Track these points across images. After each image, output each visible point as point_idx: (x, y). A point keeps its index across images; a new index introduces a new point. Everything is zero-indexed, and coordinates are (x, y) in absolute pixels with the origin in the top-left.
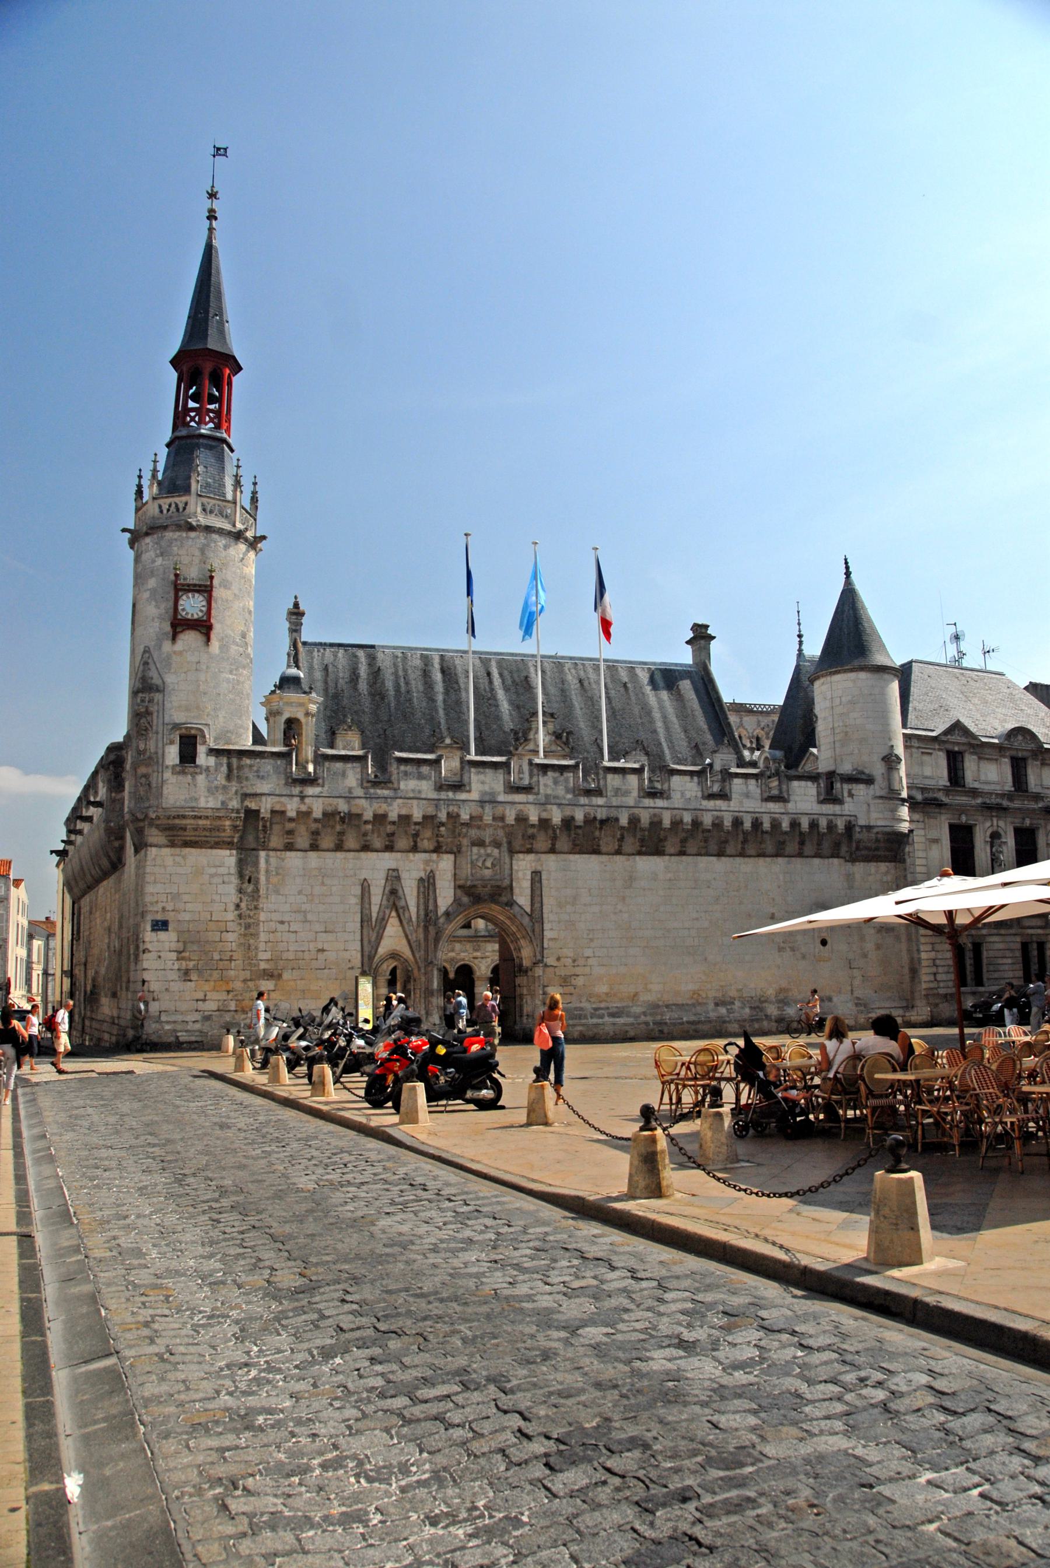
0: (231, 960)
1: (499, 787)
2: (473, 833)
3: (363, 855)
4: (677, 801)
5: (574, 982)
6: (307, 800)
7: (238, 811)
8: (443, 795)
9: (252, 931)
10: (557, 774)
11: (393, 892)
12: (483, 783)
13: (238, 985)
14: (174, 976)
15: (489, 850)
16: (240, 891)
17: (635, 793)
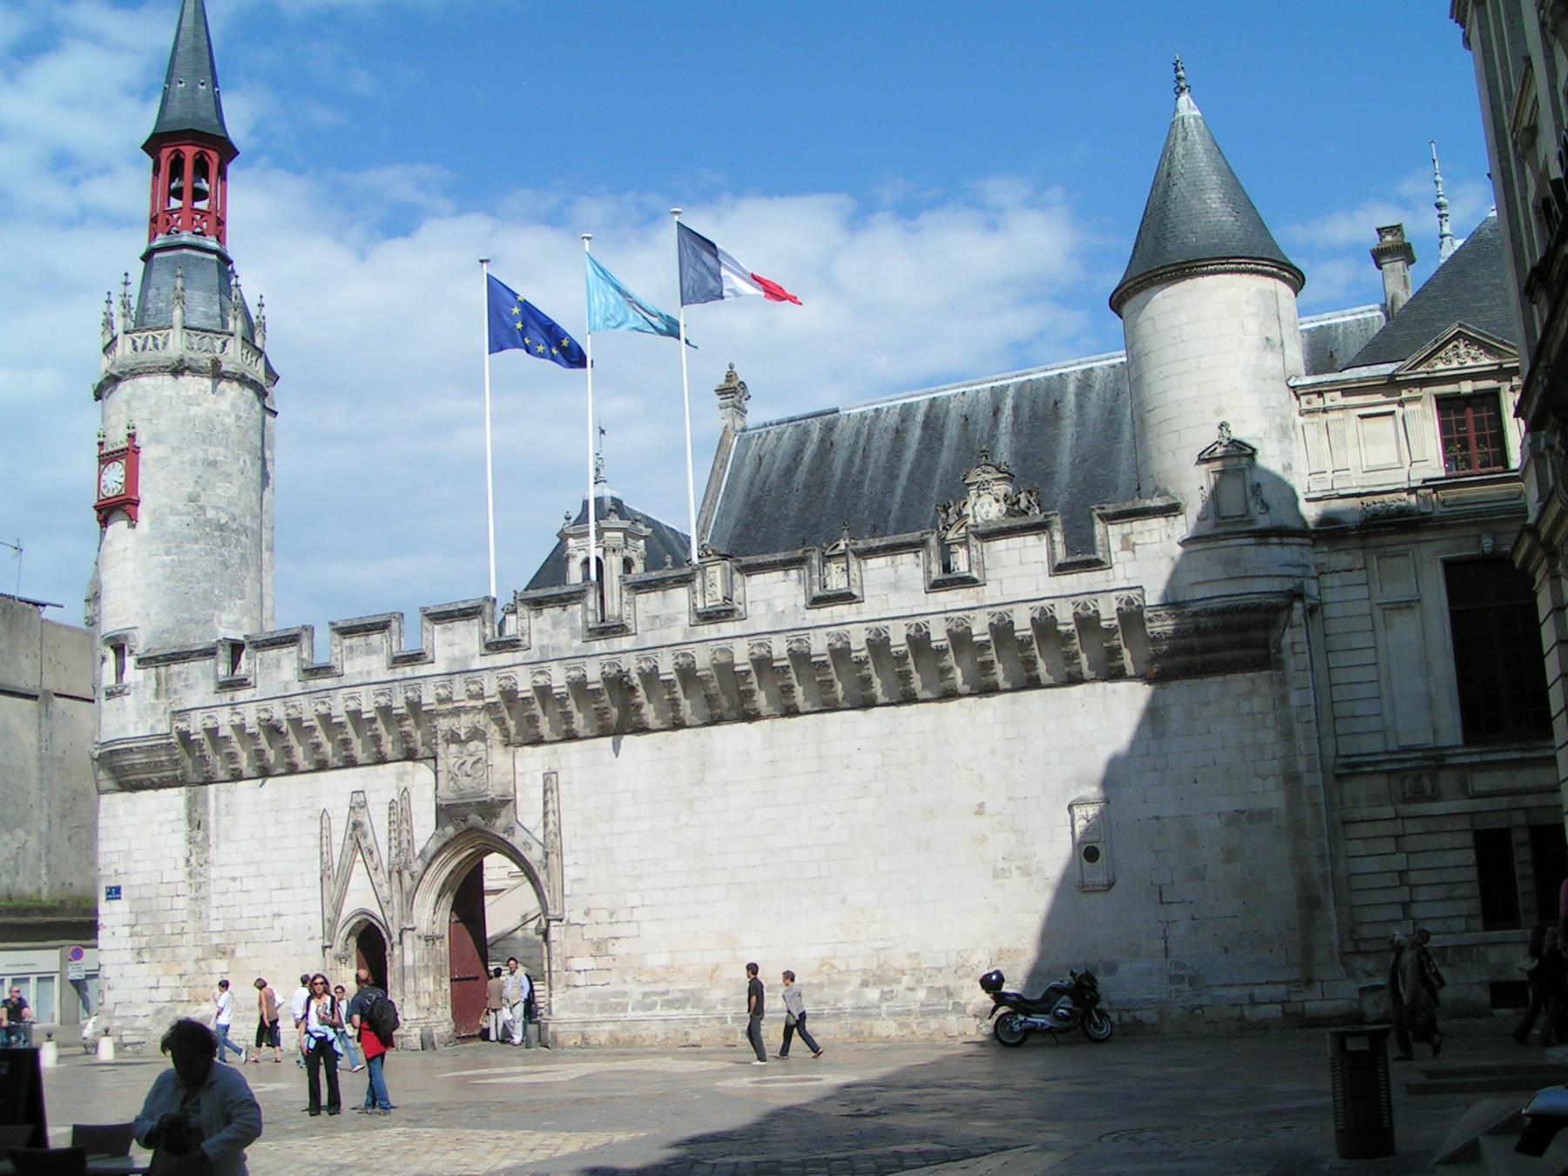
0: (182, 933)
1: (475, 646)
2: (443, 724)
3: (322, 775)
4: (758, 619)
5: (611, 950)
6: (239, 709)
7: (167, 736)
8: (401, 672)
9: (202, 892)
10: (558, 610)
11: (356, 825)
12: (451, 644)
13: (190, 966)
14: (128, 956)
15: (472, 746)
16: (191, 841)
17: (685, 619)
